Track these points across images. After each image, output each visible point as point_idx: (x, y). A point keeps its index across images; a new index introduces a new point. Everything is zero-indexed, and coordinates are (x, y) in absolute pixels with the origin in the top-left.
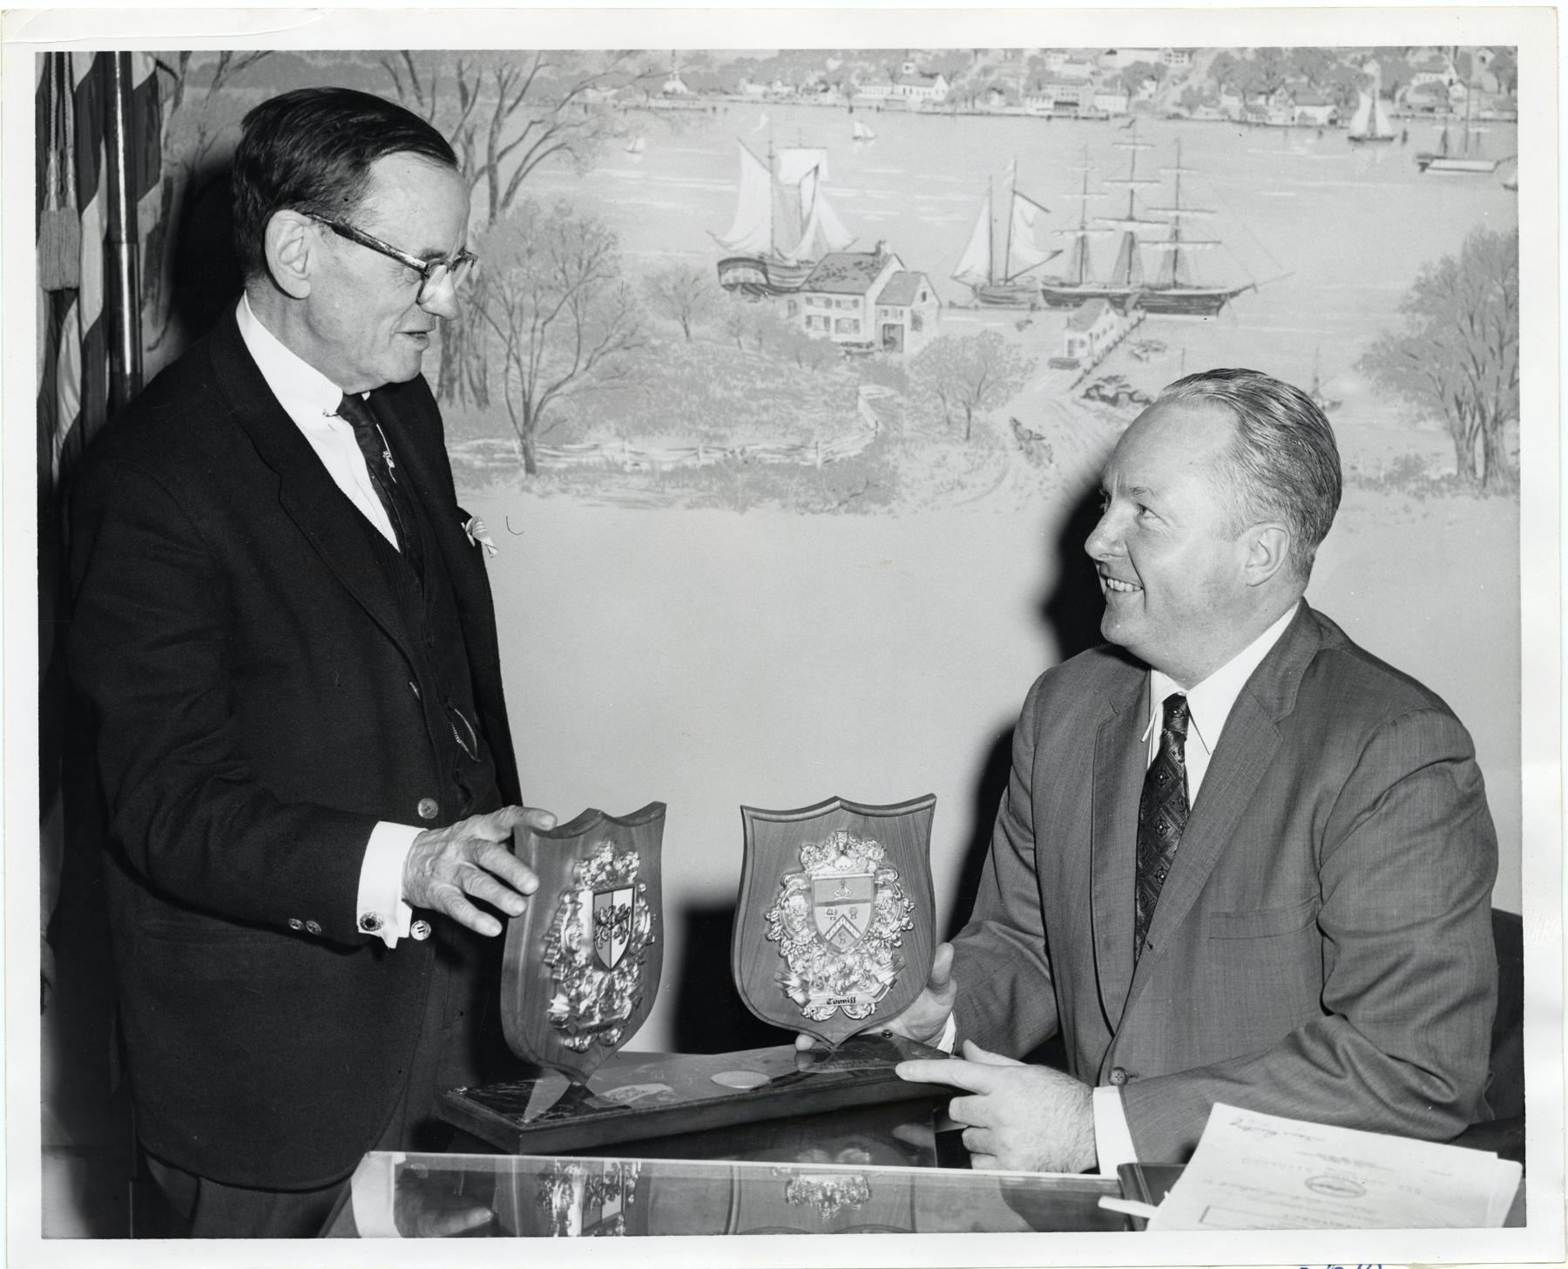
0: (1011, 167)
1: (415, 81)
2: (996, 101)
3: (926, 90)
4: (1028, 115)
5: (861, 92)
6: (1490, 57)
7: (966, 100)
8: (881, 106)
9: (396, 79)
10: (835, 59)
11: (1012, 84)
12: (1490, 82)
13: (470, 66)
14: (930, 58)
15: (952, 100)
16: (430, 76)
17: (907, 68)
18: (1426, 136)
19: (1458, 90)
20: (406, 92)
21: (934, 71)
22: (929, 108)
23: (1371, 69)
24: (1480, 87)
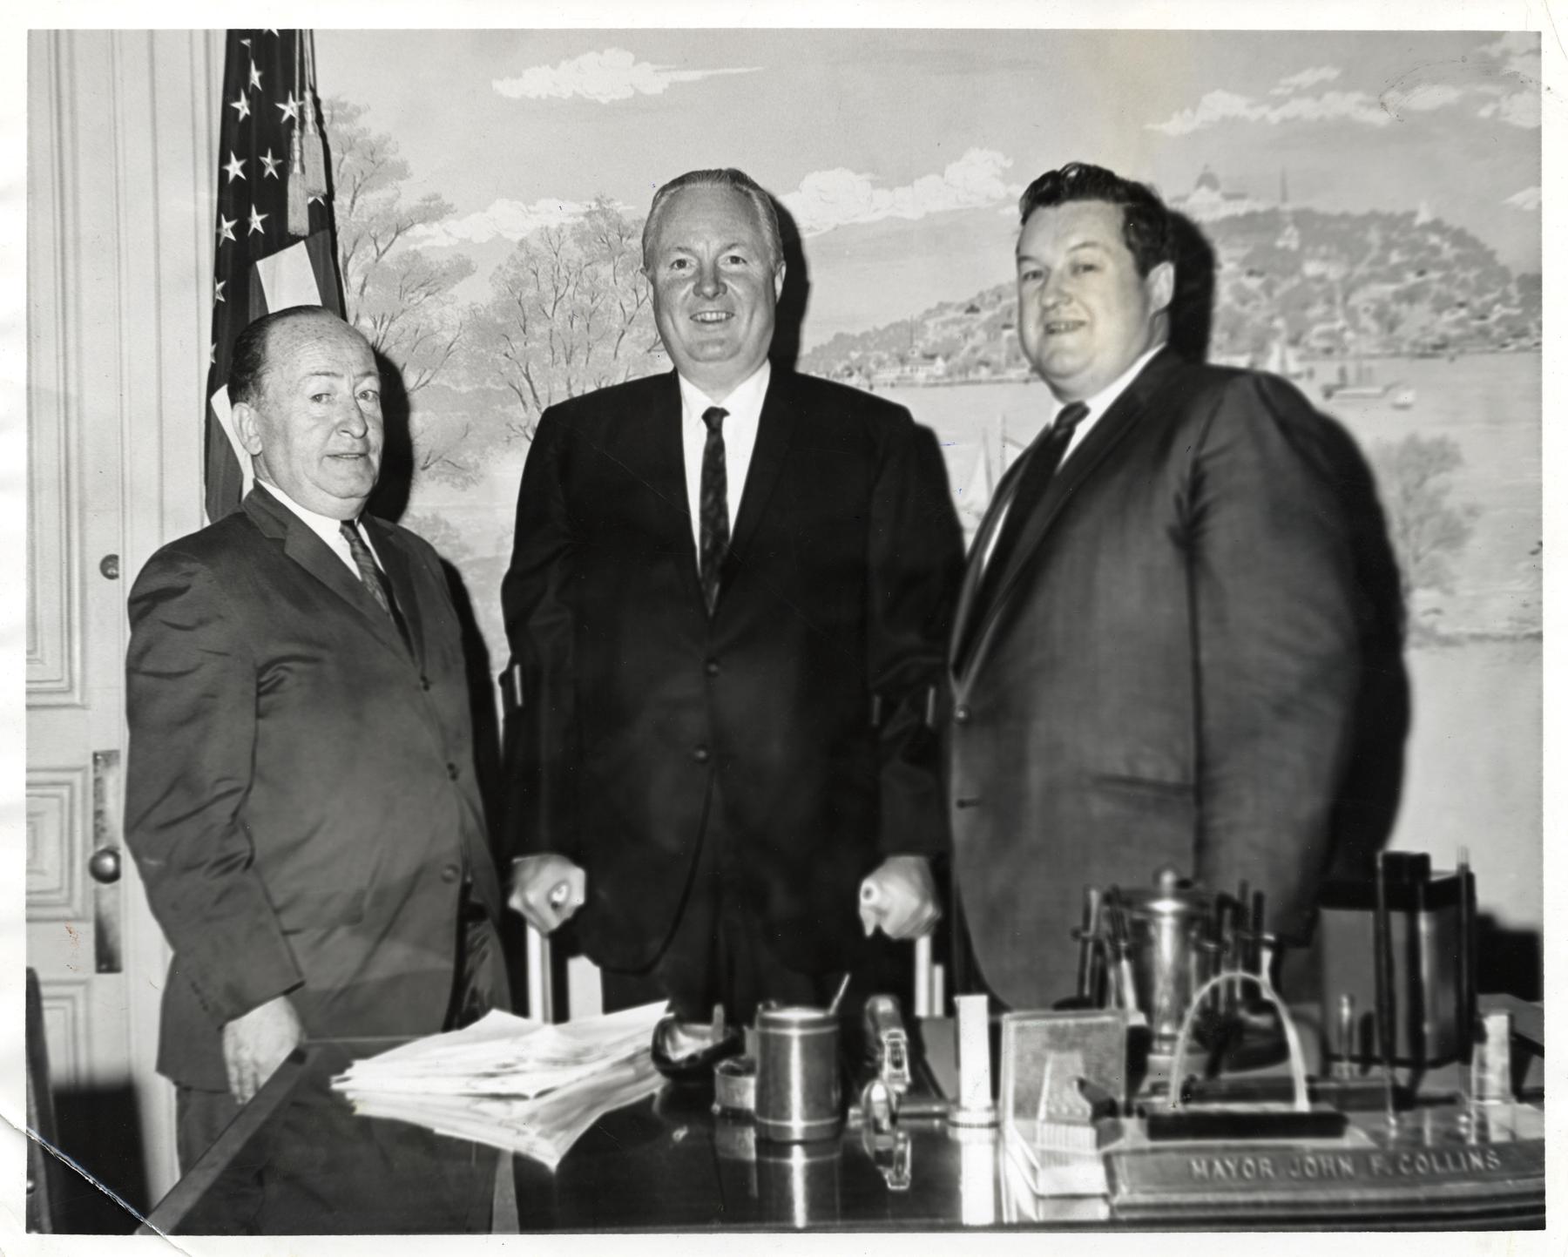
0: (999, 420)
1: (535, 396)
2: (984, 372)
3: (929, 368)
4: (1010, 381)
5: (877, 373)
6: (1373, 307)
7: (960, 372)
8: (896, 382)
9: (521, 396)
10: (855, 350)
11: (994, 357)
12: (1373, 326)
13: (577, 381)
14: (930, 344)
15: (950, 374)
16: (546, 392)
17: (913, 353)
18: (1327, 372)
19: (1349, 335)
20: (529, 405)
21: (933, 352)
22: (932, 381)
23: (1279, 323)
24: (1365, 331)
